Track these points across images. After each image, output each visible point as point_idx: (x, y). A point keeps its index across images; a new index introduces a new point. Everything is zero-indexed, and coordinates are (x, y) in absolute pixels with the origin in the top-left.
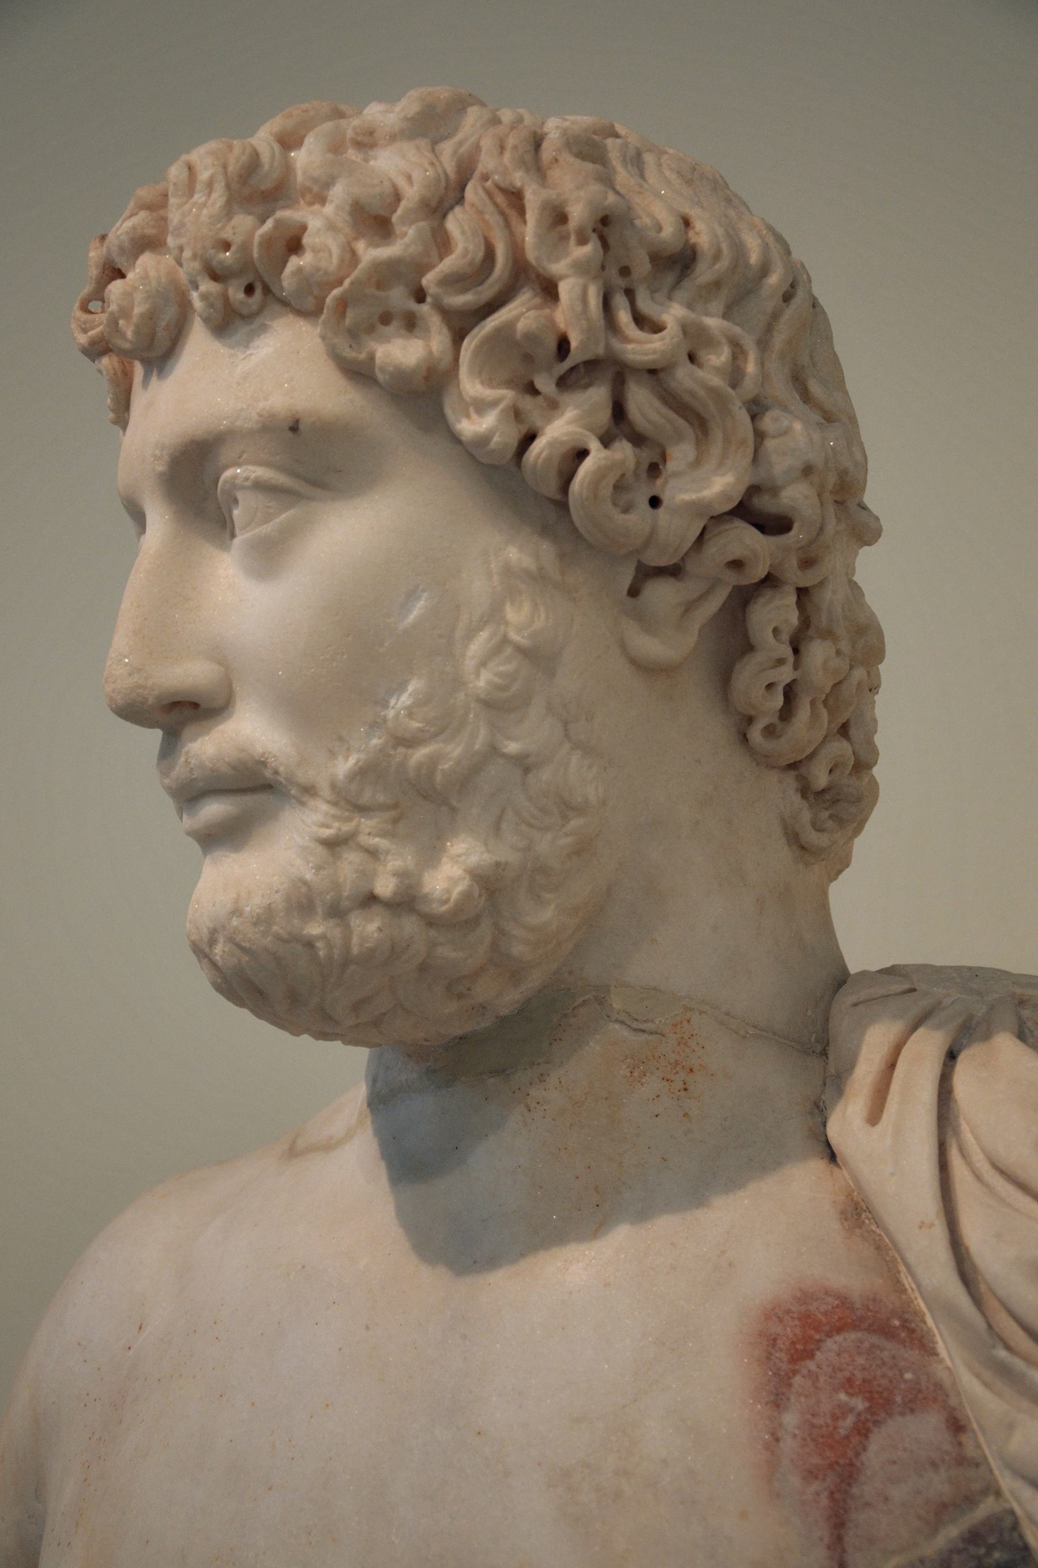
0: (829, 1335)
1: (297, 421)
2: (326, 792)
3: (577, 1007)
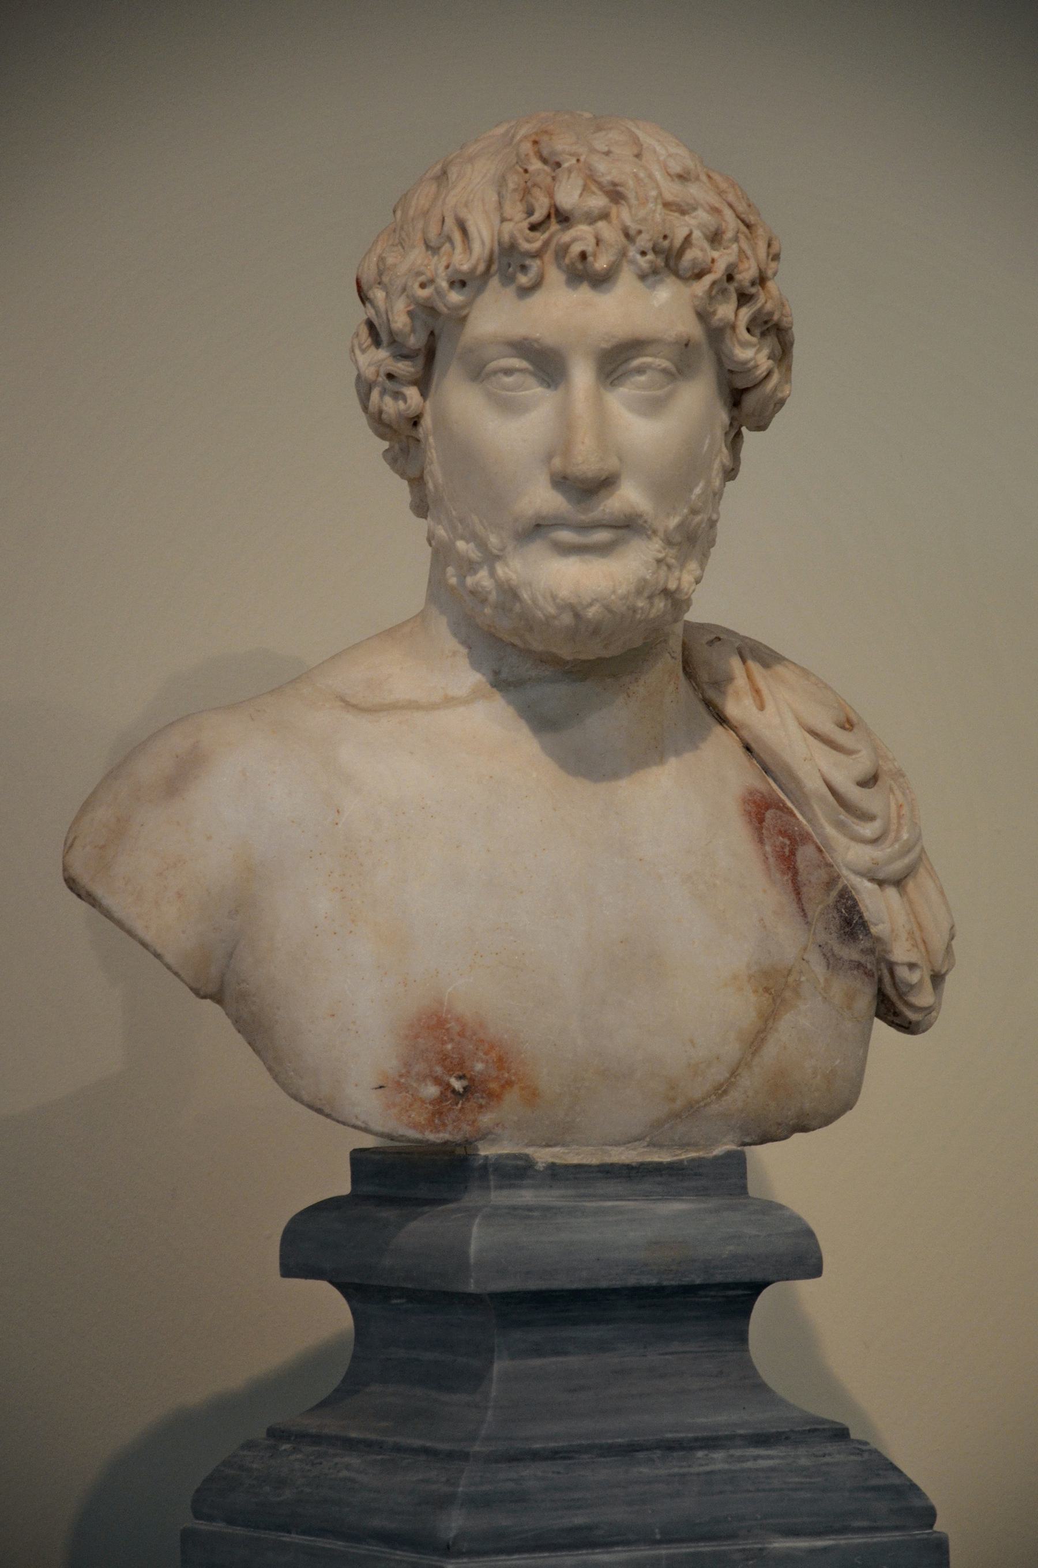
0: (766, 811)
1: (689, 341)
2: (661, 533)
3: (657, 644)
